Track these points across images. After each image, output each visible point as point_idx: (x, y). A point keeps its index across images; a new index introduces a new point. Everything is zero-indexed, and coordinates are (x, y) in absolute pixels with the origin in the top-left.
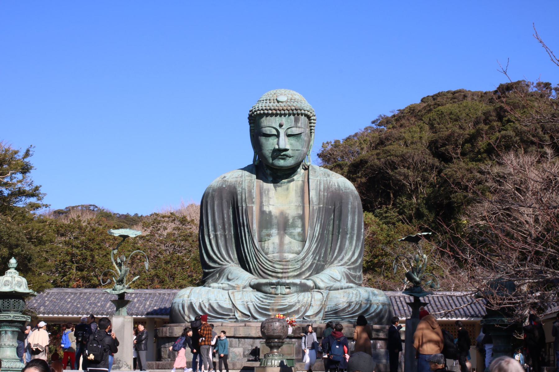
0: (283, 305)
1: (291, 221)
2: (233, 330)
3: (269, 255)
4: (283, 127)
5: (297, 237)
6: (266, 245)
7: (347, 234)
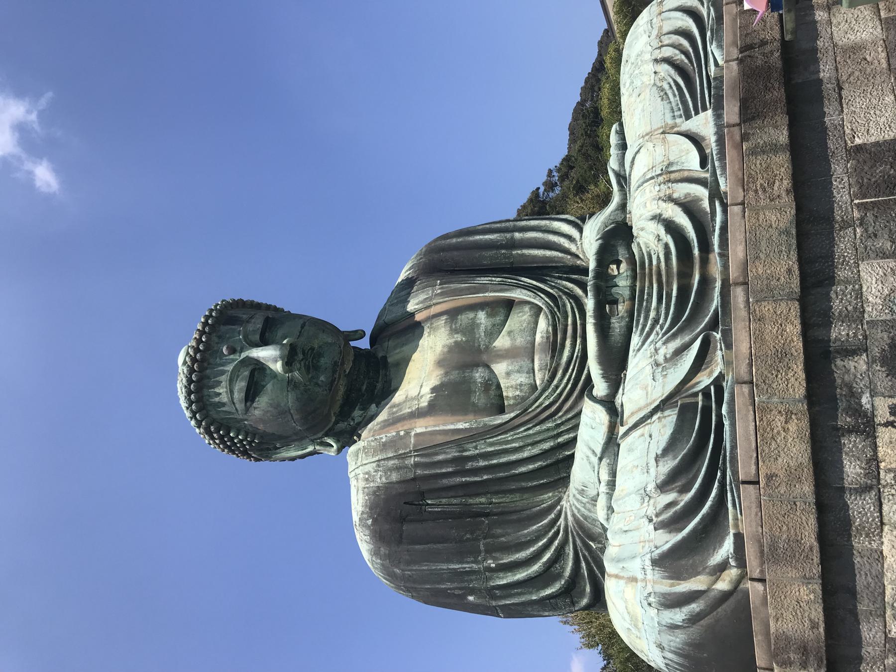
1: (459, 337)
2: (767, 308)
3: (538, 383)
5: (499, 319)
7: (512, 238)
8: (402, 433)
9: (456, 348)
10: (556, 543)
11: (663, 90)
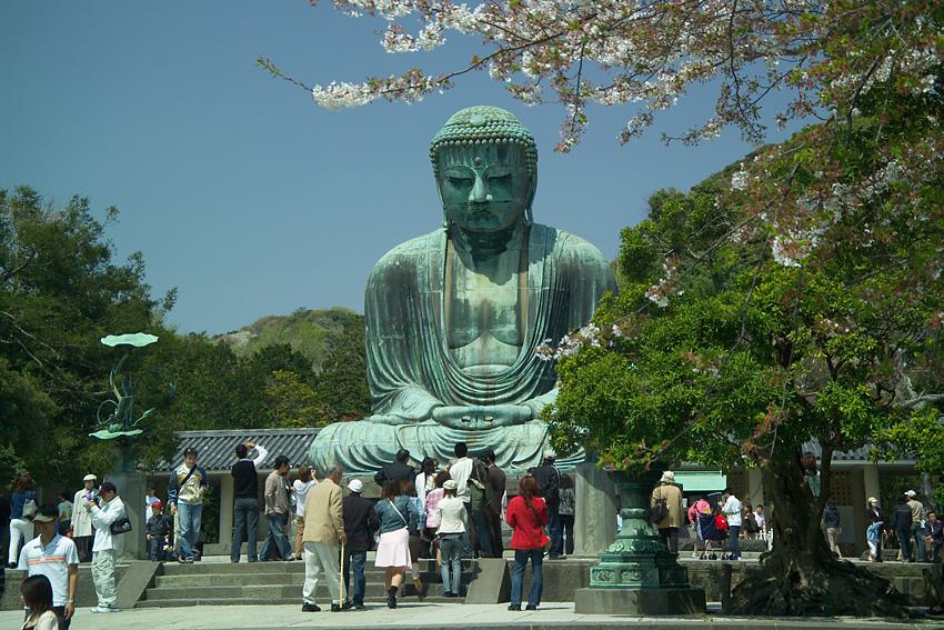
1: (498, 314)
6: (460, 352)
9: (492, 312)
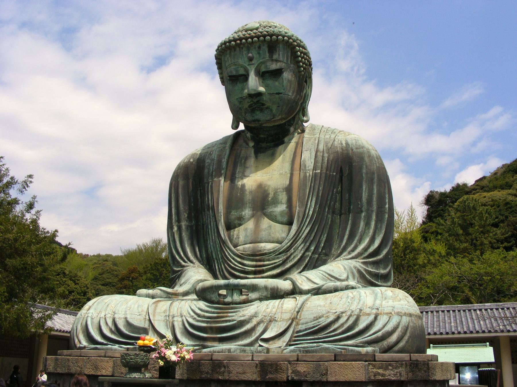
0: (229, 321)
2: (111, 364)
4: (253, 62)
6: (235, 232)
7: (362, 212)
8: (223, 172)
10: (182, 262)
11: (320, 318)
